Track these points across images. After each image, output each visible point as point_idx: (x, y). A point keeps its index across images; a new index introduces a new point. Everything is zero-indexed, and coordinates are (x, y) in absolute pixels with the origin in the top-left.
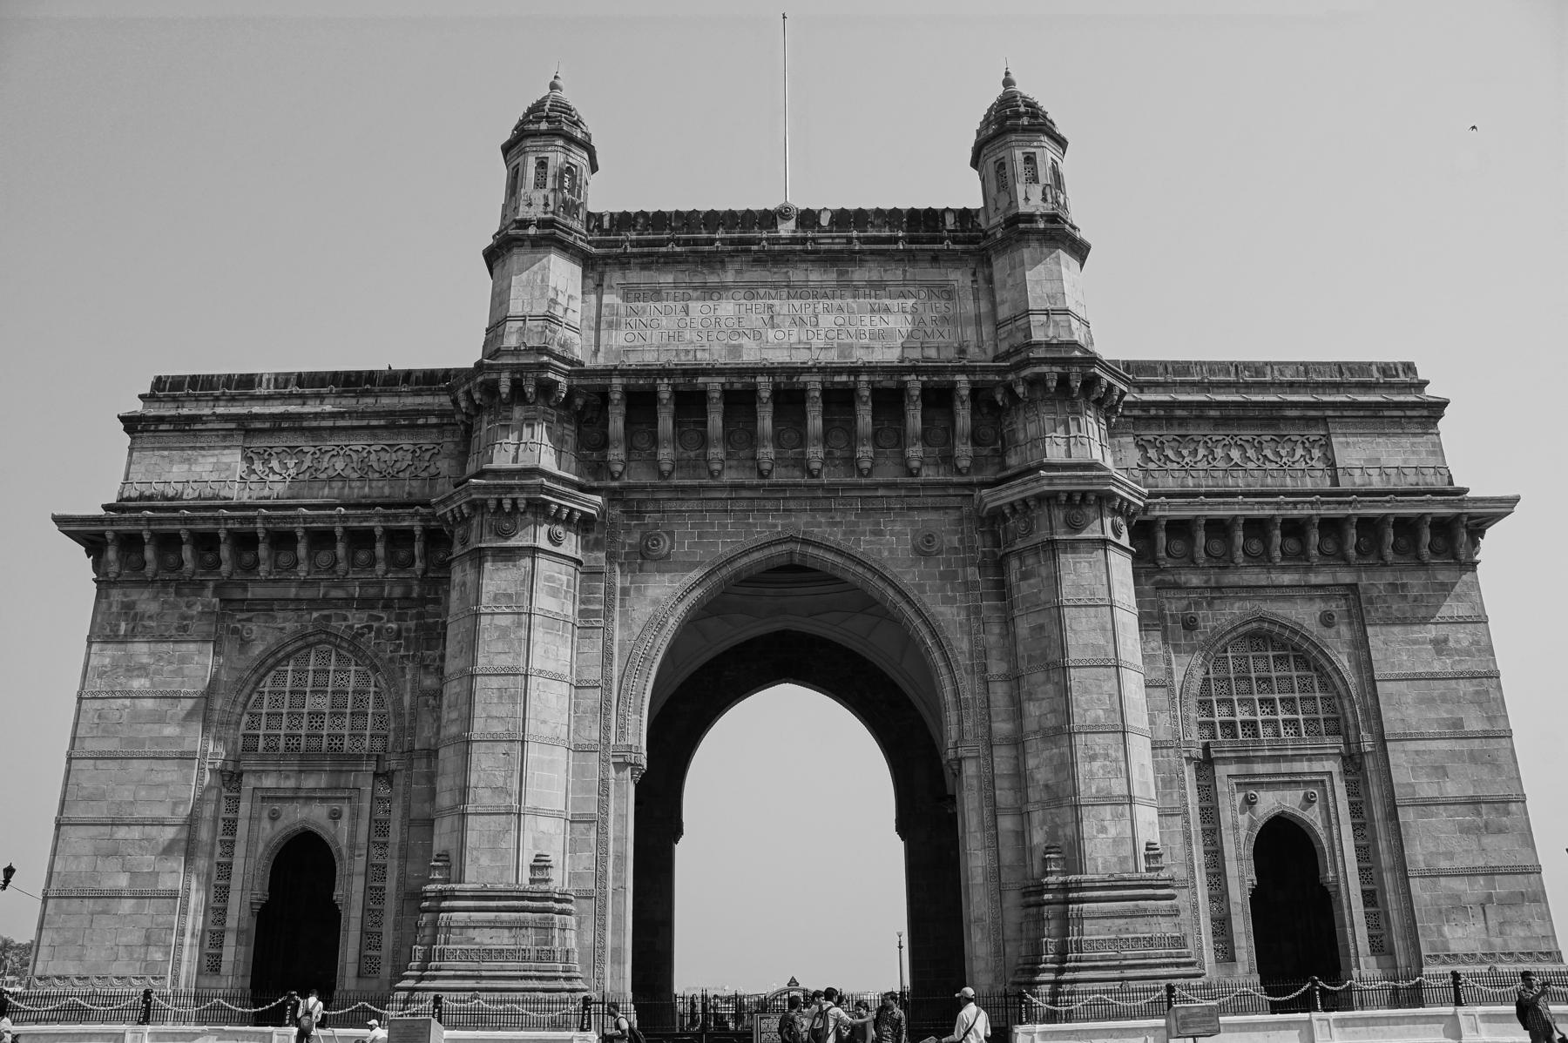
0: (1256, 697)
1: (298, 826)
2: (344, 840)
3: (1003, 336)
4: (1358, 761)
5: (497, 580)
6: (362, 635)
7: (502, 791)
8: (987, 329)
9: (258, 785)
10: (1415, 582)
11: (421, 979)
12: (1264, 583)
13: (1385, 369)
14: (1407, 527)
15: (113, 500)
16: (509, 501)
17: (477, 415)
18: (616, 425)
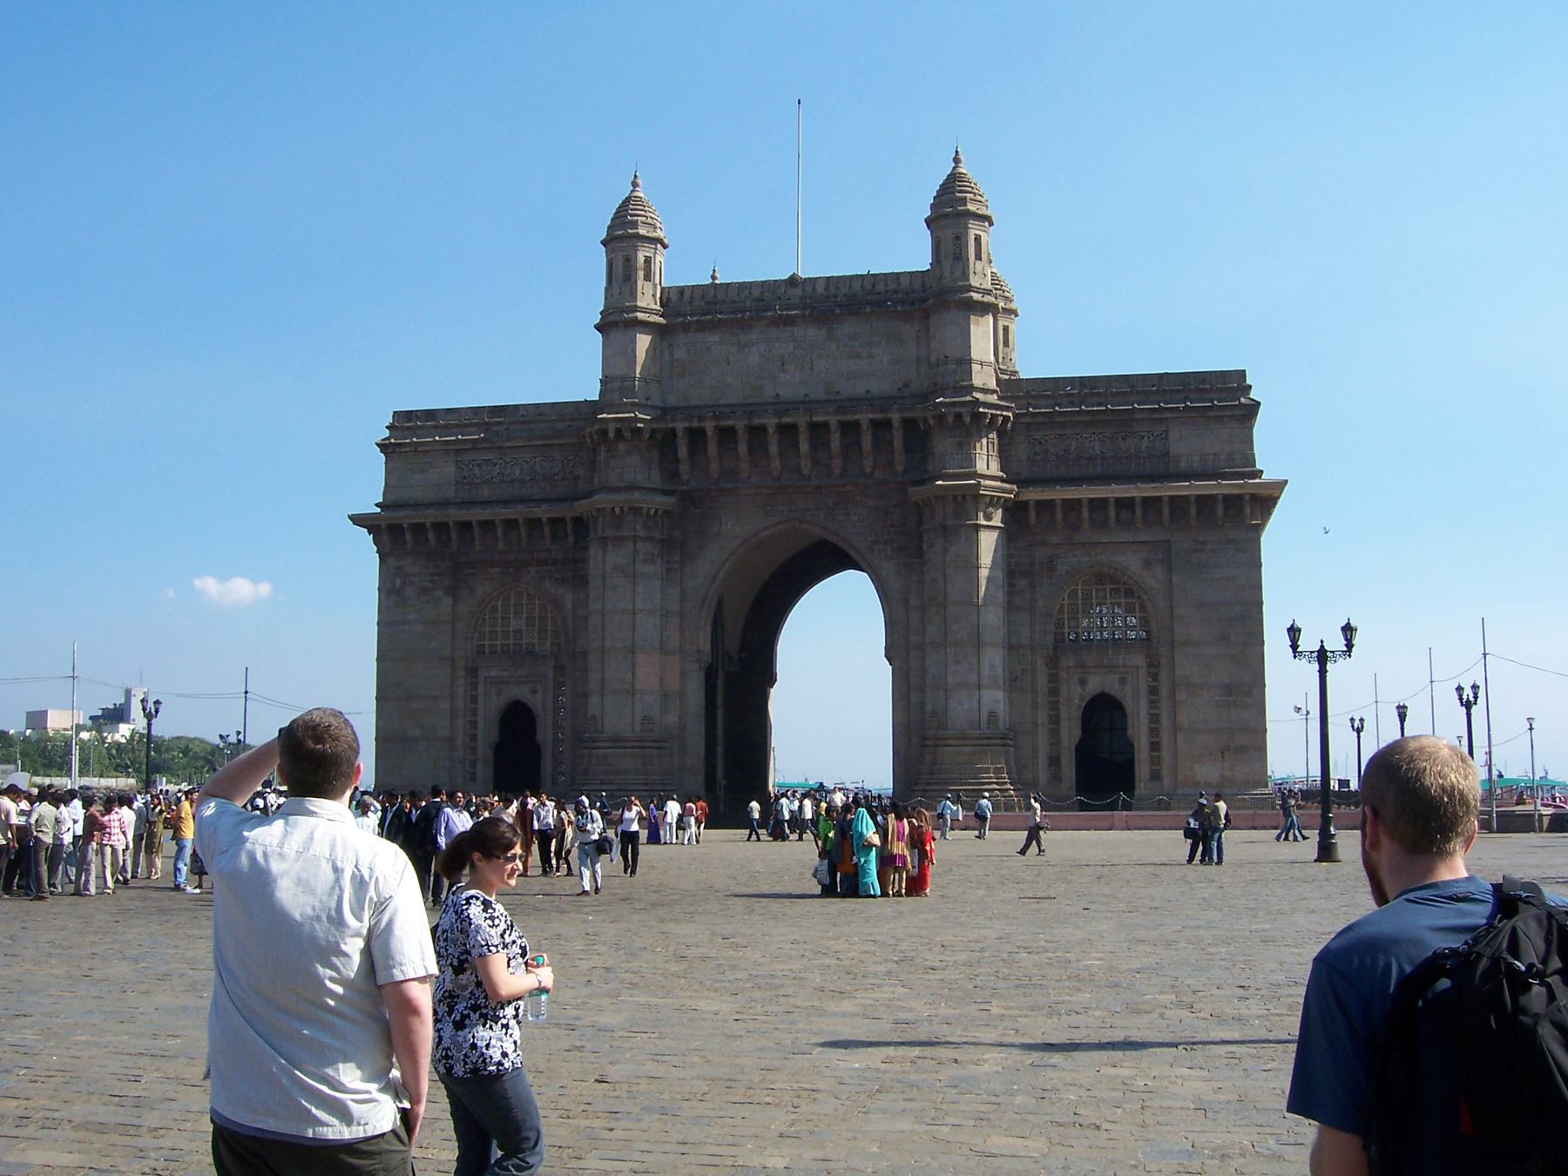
5: (616, 557)
12: (1104, 541)
14: (1205, 501)
18: (683, 451)
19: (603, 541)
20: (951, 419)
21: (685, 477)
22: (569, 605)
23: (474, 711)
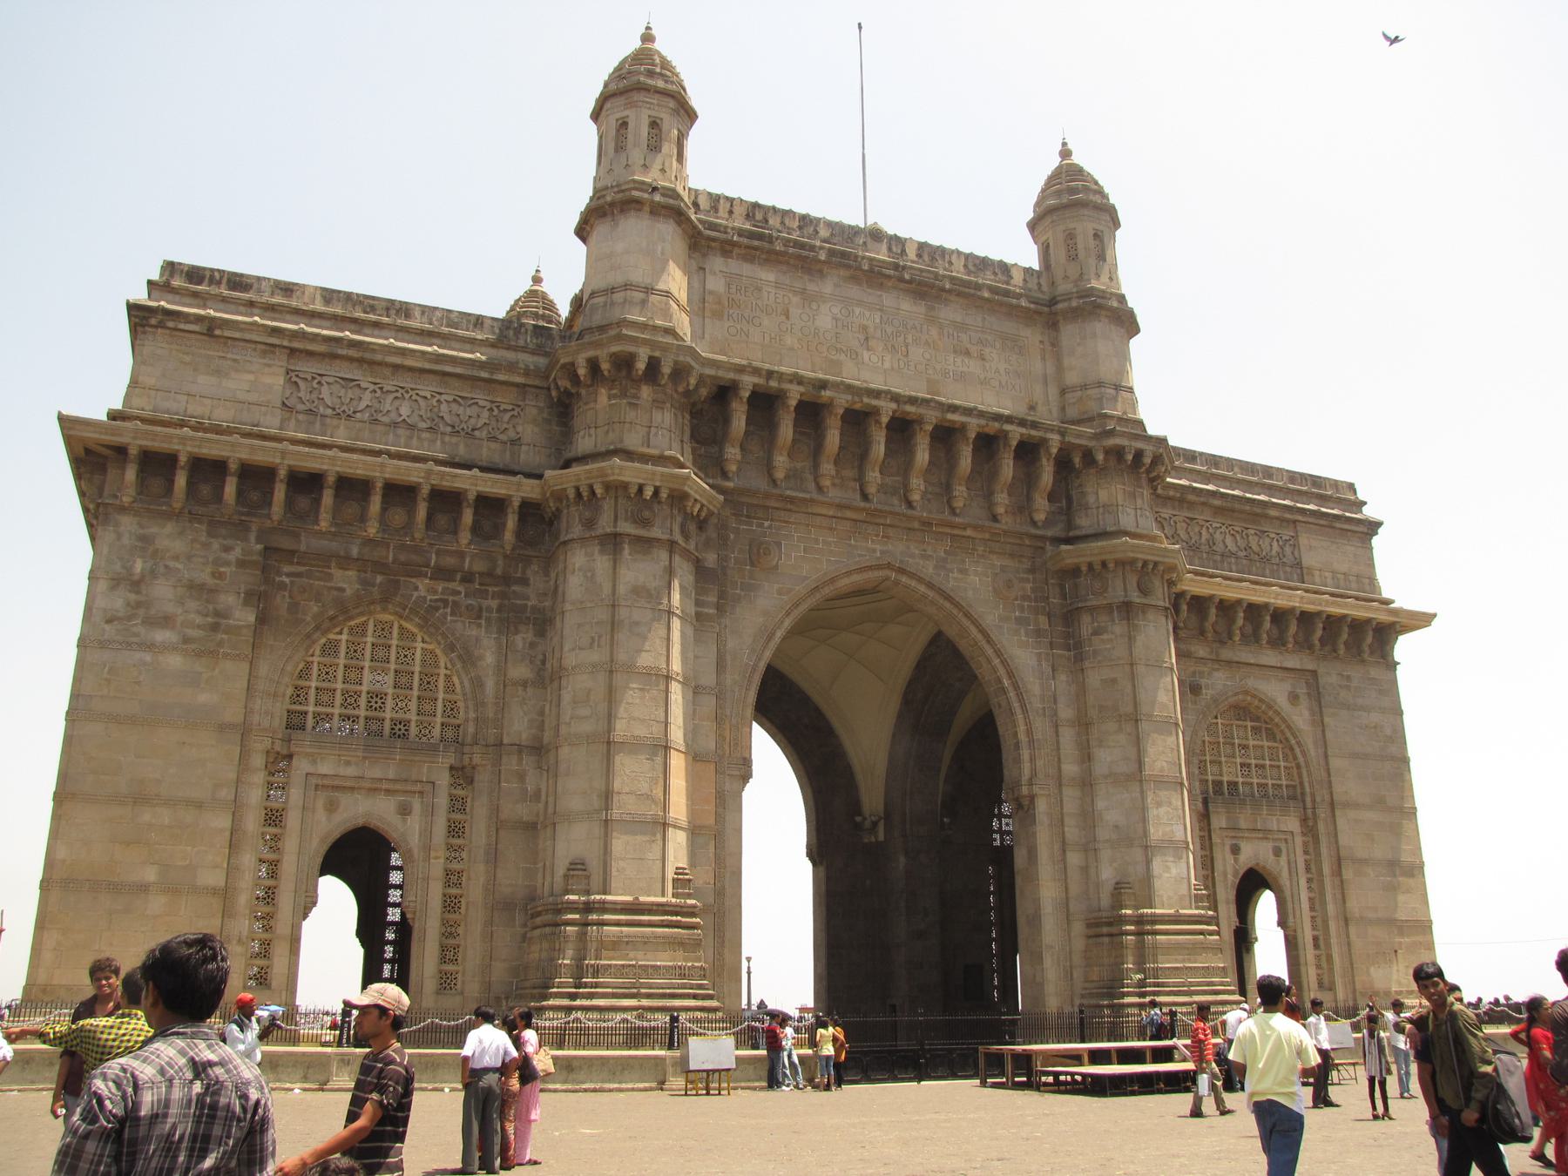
0: (1238, 760)
1: (360, 822)
2: (414, 841)
3: (1074, 400)
4: (1310, 824)
6: (437, 609)
7: (648, 797)
8: (1053, 392)
9: (312, 770)
10: (1355, 672)
11: (573, 997)
12: (1252, 661)
13: (1336, 484)
15: (118, 405)
16: (653, 489)
17: (592, 385)
20: (1130, 457)
21: (734, 468)
22: (489, 659)
23: (275, 843)
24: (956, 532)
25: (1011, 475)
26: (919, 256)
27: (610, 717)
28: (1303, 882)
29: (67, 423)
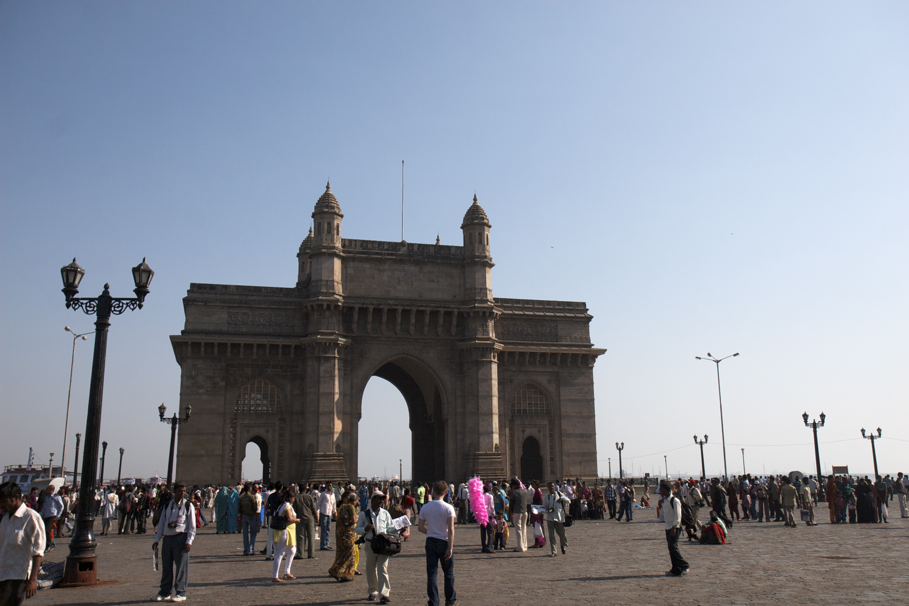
0: (528, 402)
13: (577, 304)
14: (574, 356)
18: (356, 317)
19: (318, 359)
22: (288, 389)
23: (234, 441)
24: (425, 341)
25: (442, 322)
26: (418, 249)
27: (318, 406)
28: (548, 441)
29: (172, 338)
